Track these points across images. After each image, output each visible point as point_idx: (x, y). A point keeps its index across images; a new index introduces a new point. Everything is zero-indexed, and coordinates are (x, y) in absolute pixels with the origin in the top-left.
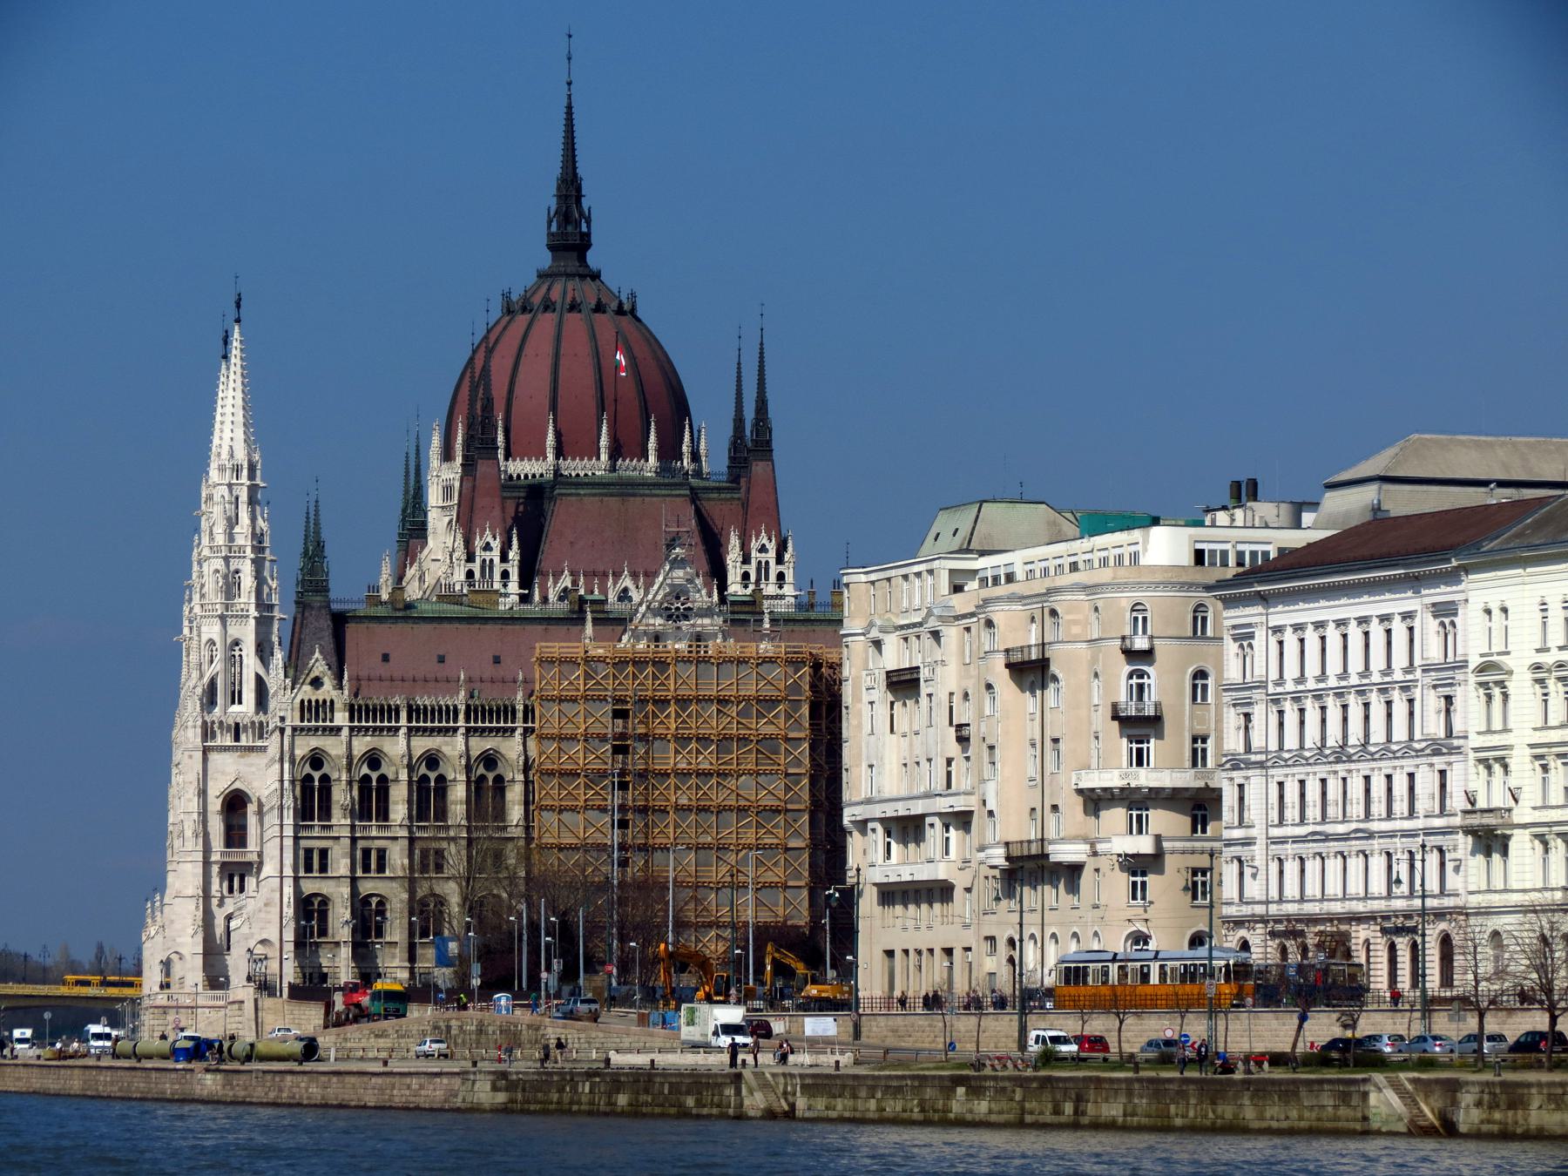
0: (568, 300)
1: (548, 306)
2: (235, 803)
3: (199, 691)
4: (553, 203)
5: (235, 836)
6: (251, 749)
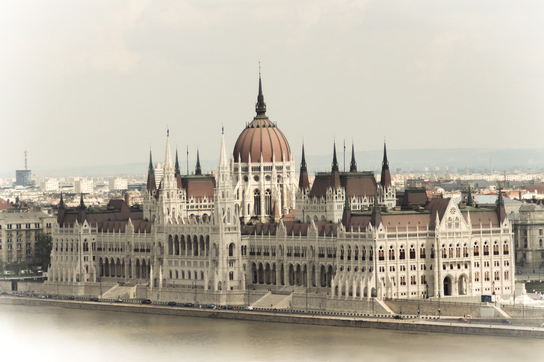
1: (264, 126)
5: (231, 254)
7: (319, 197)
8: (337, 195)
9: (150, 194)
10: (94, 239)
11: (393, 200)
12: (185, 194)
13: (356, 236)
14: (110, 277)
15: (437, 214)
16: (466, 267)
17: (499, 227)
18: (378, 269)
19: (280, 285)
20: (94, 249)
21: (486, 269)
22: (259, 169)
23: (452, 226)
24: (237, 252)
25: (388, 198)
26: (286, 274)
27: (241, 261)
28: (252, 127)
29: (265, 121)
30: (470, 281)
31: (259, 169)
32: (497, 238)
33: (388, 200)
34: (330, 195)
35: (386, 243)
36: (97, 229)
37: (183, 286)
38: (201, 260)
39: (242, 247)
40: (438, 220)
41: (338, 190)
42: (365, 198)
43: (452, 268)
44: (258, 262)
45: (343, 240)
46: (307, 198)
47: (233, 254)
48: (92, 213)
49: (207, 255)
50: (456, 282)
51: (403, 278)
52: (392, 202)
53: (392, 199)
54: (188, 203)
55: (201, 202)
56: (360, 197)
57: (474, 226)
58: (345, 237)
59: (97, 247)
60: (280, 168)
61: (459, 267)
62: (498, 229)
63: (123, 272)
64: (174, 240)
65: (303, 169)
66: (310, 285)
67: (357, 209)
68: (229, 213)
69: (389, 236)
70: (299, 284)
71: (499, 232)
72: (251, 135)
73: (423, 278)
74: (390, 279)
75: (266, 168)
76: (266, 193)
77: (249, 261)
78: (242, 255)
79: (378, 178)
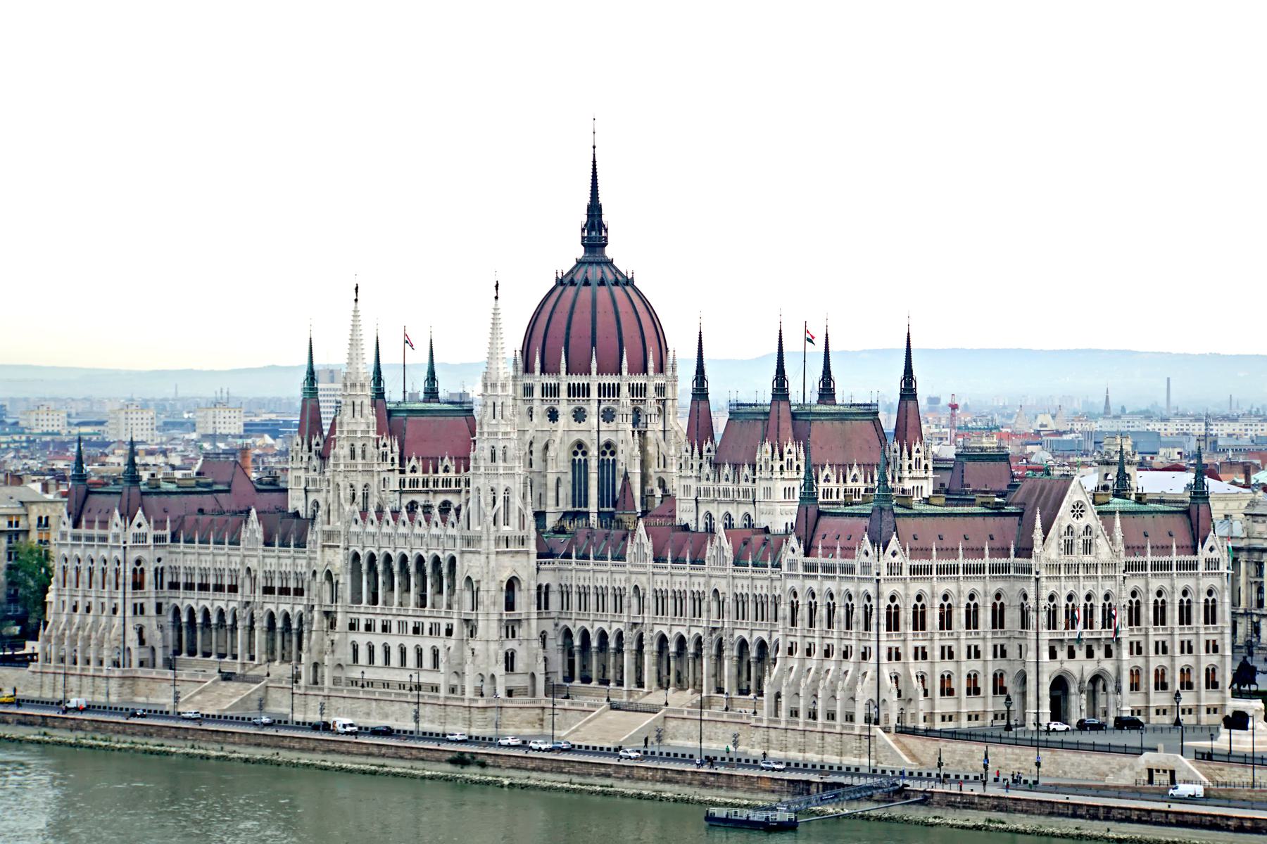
0: (599, 277)
1: (602, 283)
2: (512, 584)
3: (491, 519)
4: (585, 219)
5: (510, 605)
6: (518, 552)
7: (736, 467)
8: (784, 463)
9: (306, 447)
10: (159, 560)
11: (927, 478)
12: (396, 449)
13: (829, 568)
14: (199, 656)
15: (1038, 516)
16: (1108, 654)
17: (1196, 553)
18: (884, 653)
19: (633, 687)
20: (159, 585)
21: (1157, 661)
22: (586, 390)
23: (1075, 549)
24: (525, 601)
25: (914, 474)
26: (649, 660)
27: (534, 623)
28: (572, 283)
29: (606, 269)
30: (1118, 690)
31: (586, 390)
32: (1190, 582)
33: (913, 478)
34: (766, 463)
35: (906, 588)
36: (168, 532)
37: (386, 685)
38: (432, 620)
39: (539, 587)
40: (1038, 534)
41: (786, 450)
42: (855, 471)
43: (1071, 654)
44: (578, 627)
45: (797, 576)
46: (707, 469)
47: (517, 605)
48: (156, 493)
49: (449, 606)
50: (1081, 692)
51: (946, 679)
52: (924, 483)
53: (924, 475)
54: (402, 472)
55: (436, 471)
56: (842, 469)
57: (1130, 549)
58: (800, 571)
59: (167, 579)
60: (638, 391)
61: (1090, 654)
62: (1193, 558)
63: (234, 646)
64: (365, 567)
65: (700, 393)
66: (709, 691)
67: (834, 499)
68: (506, 500)
69: (913, 570)
70: (681, 684)
71: (1194, 566)
72: (568, 306)
73: (998, 679)
74: (914, 679)
75: (602, 390)
76: (604, 453)
77: (556, 625)
78: (539, 608)
79: (889, 422)
